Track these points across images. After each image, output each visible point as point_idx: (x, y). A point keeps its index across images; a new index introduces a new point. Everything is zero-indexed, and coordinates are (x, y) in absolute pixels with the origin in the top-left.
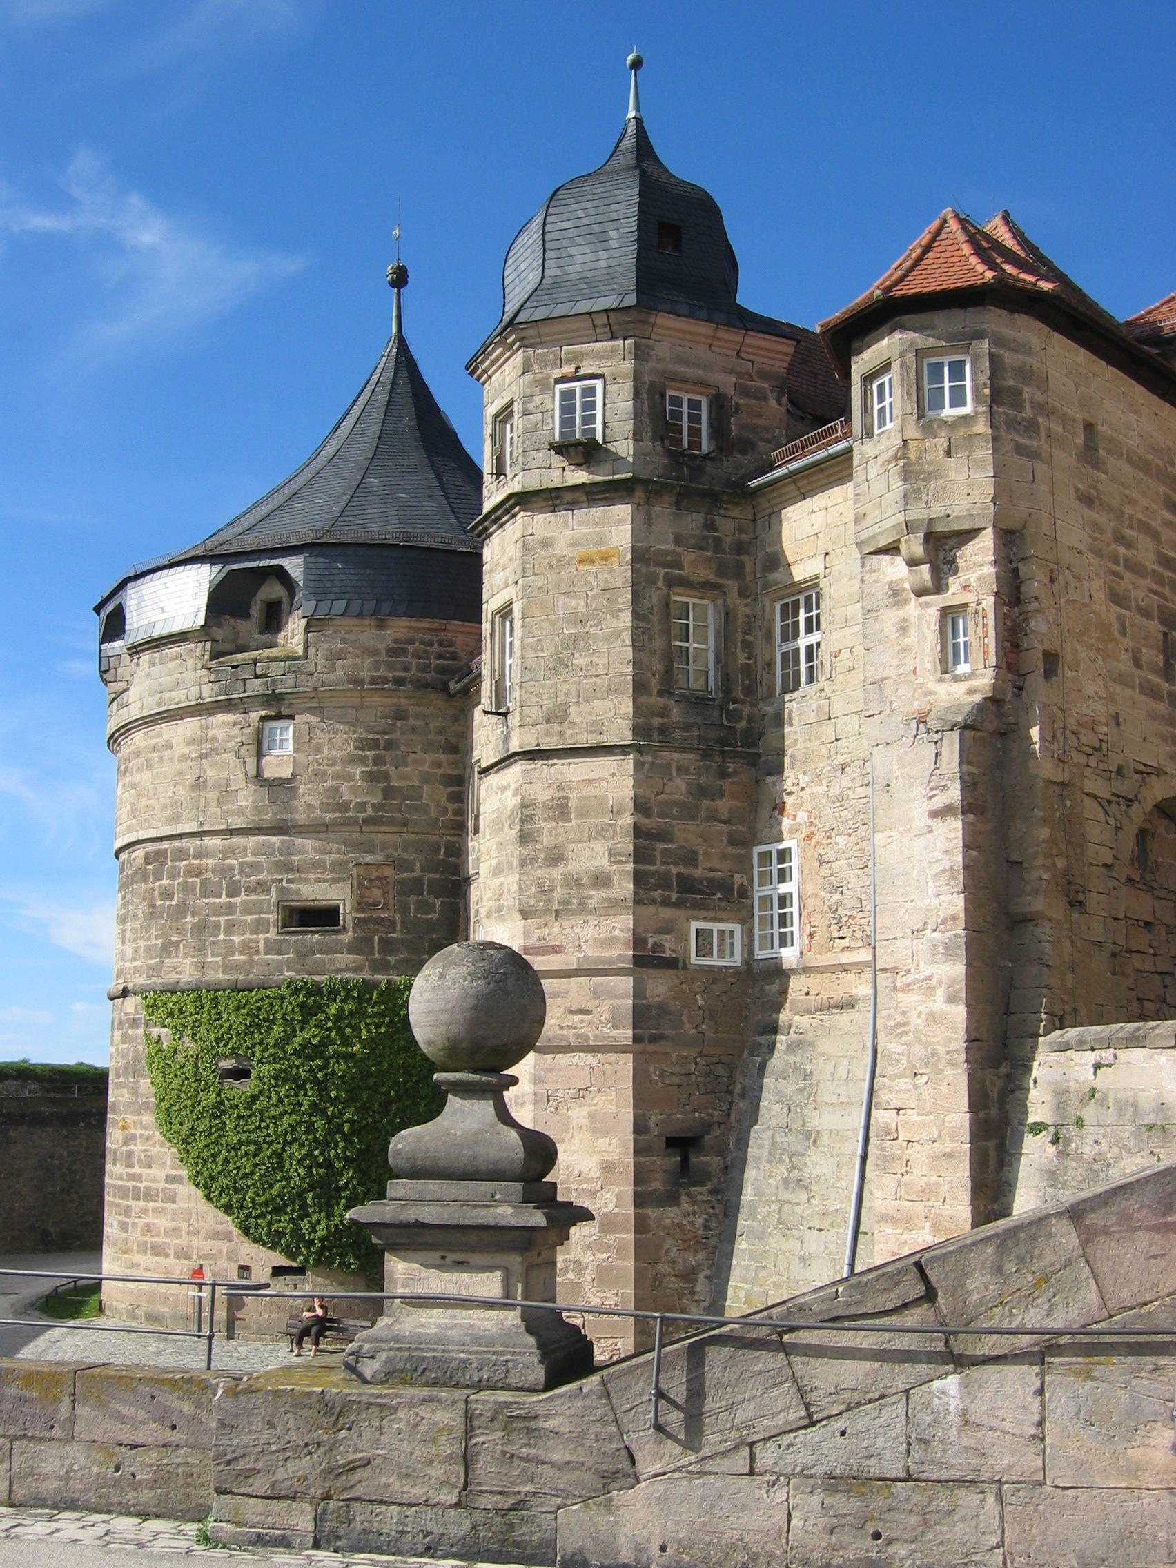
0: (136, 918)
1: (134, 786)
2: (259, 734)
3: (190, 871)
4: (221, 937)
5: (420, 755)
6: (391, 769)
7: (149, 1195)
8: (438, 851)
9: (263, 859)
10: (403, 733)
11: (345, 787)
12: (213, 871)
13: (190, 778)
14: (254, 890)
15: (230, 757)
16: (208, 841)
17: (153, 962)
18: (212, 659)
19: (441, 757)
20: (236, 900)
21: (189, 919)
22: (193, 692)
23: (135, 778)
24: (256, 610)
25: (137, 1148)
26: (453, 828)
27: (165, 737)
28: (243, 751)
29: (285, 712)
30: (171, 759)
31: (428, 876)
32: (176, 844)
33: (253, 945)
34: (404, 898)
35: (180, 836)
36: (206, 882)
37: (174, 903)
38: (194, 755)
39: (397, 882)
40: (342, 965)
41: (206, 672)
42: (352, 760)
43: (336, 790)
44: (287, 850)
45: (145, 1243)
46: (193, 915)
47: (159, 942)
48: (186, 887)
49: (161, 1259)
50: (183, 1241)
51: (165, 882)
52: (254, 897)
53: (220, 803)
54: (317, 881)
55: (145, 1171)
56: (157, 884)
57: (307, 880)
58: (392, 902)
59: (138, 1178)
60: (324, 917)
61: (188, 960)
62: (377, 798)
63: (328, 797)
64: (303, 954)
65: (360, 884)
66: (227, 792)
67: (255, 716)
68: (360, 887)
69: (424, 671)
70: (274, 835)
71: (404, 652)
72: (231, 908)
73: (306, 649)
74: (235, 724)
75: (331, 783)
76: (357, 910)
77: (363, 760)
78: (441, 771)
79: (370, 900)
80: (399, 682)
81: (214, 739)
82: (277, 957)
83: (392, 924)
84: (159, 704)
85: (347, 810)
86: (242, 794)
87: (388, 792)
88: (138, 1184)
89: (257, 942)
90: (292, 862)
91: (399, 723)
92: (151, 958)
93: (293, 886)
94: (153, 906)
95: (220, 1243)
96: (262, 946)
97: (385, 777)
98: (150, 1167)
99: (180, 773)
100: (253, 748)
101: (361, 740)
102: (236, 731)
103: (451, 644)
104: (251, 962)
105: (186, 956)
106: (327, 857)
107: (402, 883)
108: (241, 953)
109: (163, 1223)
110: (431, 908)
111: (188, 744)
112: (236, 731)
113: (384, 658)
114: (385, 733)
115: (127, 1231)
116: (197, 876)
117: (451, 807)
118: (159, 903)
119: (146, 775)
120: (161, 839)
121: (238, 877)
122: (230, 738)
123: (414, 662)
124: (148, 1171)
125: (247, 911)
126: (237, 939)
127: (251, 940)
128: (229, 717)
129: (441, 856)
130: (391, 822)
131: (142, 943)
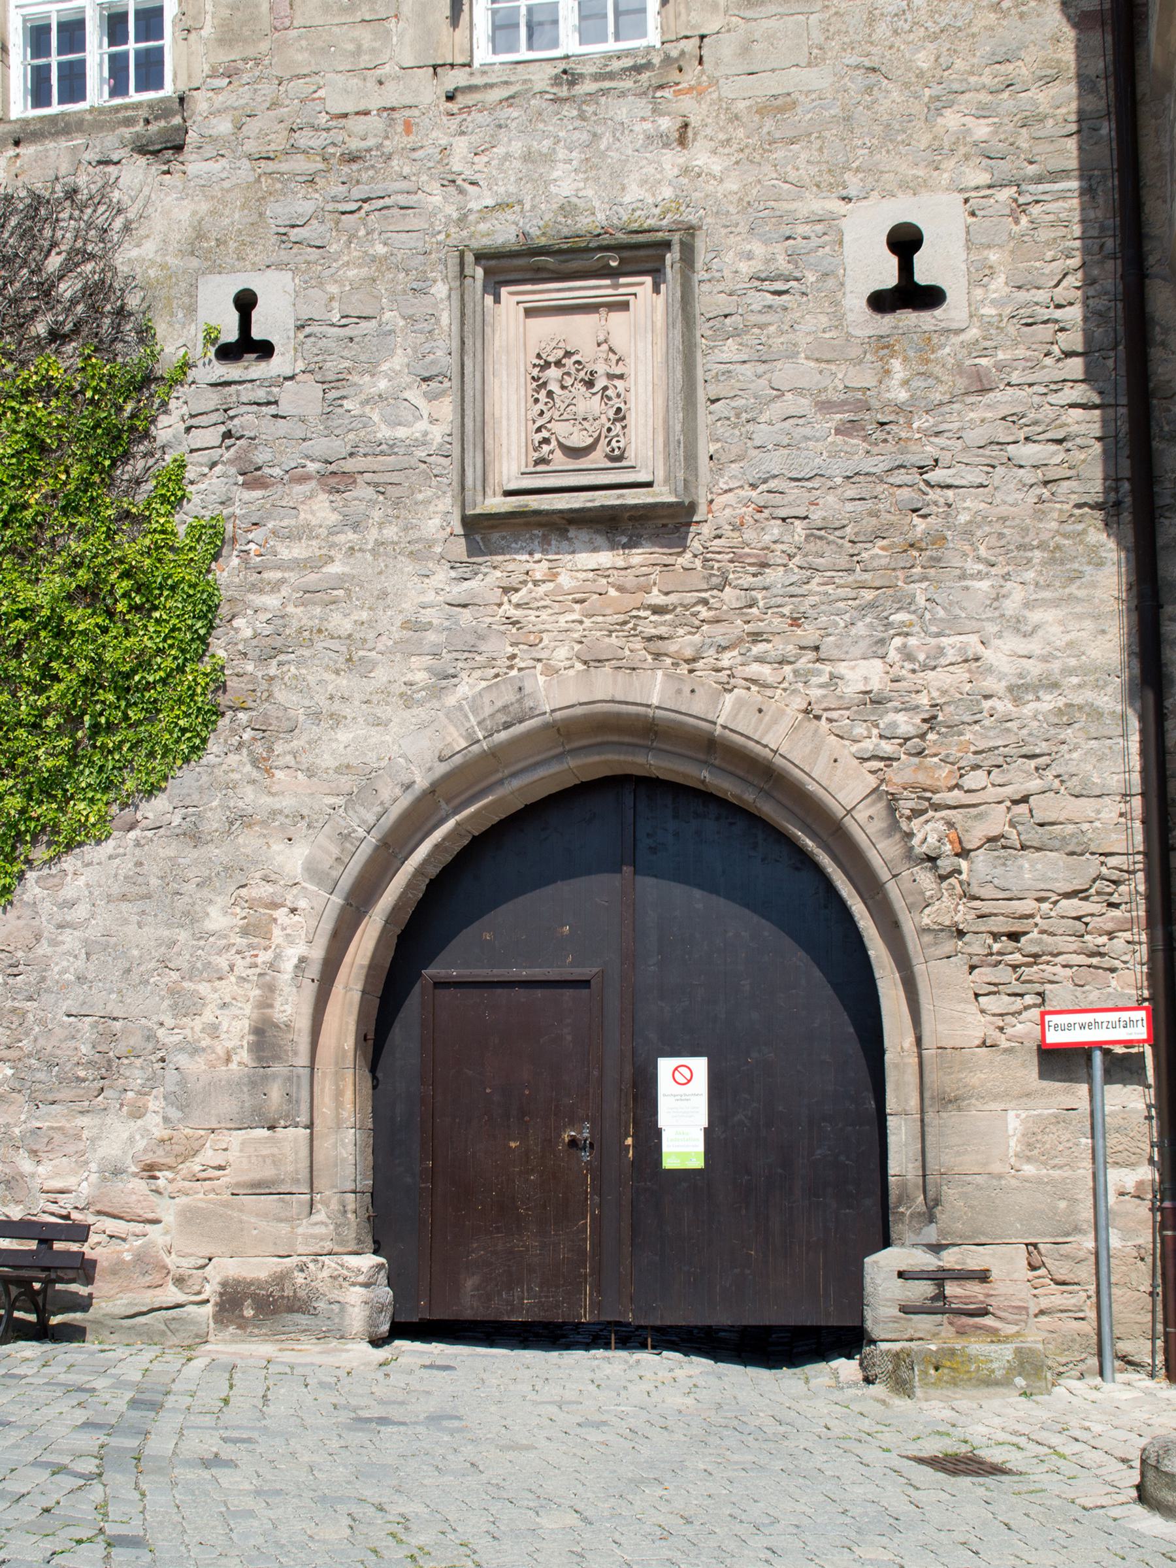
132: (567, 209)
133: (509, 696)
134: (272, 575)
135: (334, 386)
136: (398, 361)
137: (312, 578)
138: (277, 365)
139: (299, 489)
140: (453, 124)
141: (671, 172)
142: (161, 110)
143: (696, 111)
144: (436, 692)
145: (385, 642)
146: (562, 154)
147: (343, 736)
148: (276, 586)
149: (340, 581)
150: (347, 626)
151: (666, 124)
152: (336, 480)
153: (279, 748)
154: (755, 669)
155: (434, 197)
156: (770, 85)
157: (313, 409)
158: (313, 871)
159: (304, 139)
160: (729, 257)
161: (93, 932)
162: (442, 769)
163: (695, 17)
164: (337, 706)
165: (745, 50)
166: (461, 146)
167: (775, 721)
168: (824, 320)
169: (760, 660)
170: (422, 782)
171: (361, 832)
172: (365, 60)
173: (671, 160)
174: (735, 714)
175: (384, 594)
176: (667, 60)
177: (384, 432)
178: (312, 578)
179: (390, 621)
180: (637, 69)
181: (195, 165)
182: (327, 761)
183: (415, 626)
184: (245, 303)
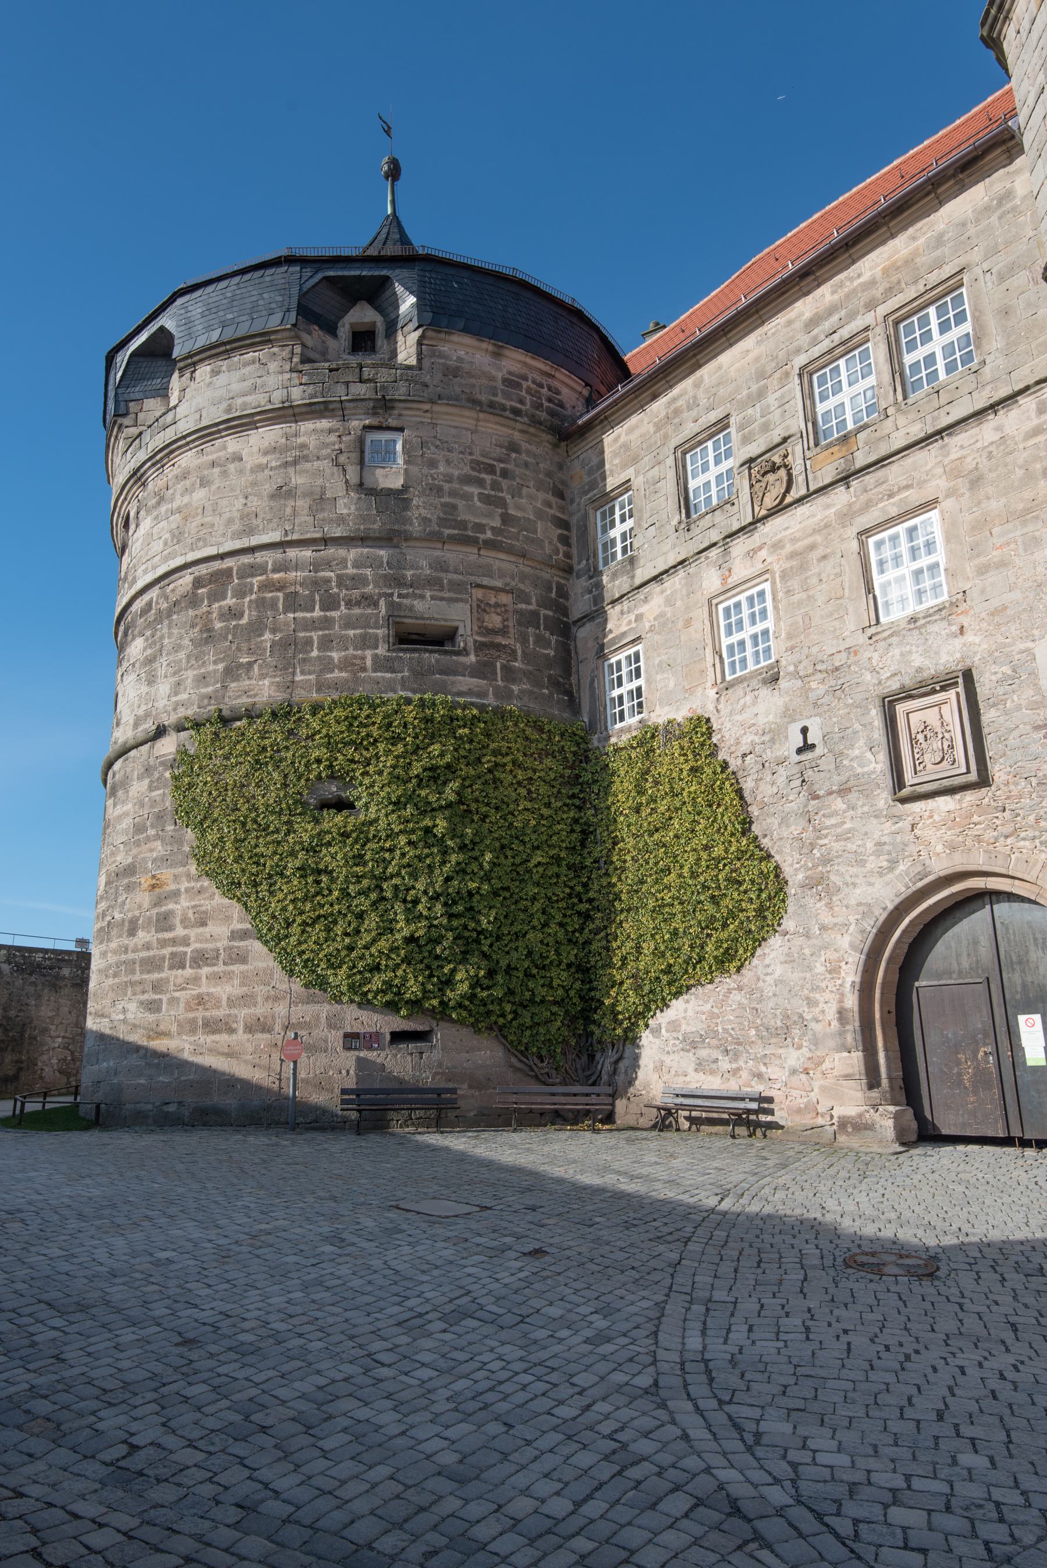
0: (177, 648)
1: (179, 510)
2: (361, 441)
3: (264, 587)
4: (315, 653)
5: (533, 491)
6: (508, 497)
7: (201, 959)
8: (550, 589)
9: (368, 572)
10: (517, 466)
11: (461, 504)
12: (301, 585)
13: (269, 488)
14: (358, 603)
15: (325, 465)
16: (292, 553)
17: (210, 689)
18: (303, 362)
19: (550, 497)
20: (335, 614)
21: (267, 636)
22: (278, 397)
24: (344, 330)
25: (181, 906)
26: (564, 570)
27: (230, 450)
28: (342, 459)
29: (392, 422)
31: (543, 612)
32: (246, 559)
33: (358, 662)
34: (523, 629)
35: (252, 550)
36: (287, 596)
37: (244, 621)
38: (274, 464)
39: (516, 611)
40: (464, 688)
41: (295, 375)
42: (466, 480)
43: (454, 507)
44: (397, 564)
45: (194, 1021)
46: (274, 631)
47: (221, 667)
48: (261, 604)
49: (223, 1038)
50: (260, 1010)
51: (230, 601)
52: (357, 611)
53: (312, 512)
54: (432, 598)
55: (193, 933)
56: (216, 605)
57: (422, 597)
58: (512, 630)
59: (185, 941)
60: (441, 639)
61: (266, 682)
62: (497, 523)
63: (445, 513)
64: (420, 673)
65: (479, 606)
66: (320, 501)
67: (356, 424)
68: (482, 608)
69: (537, 408)
70: (381, 547)
71: (518, 386)
72: (326, 623)
73: (420, 360)
74: (330, 431)
75: (446, 499)
76: (478, 634)
77: (481, 483)
78: (552, 512)
79: (490, 626)
80: (516, 412)
81: (303, 446)
82: (388, 675)
83: (514, 652)
84: (229, 410)
85: (465, 529)
86: (340, 503)
87: (506, 519)
88: (181, 949)
89: (363, 658)
90: (404, 576)
91: (514, 455)
92: (207, 686)
93: (406, 601)
95: (317, 1007)
96: (369, 662)
97: (503, 504)
98: (203, 924)
99: (254, 484)
100: (354, 456)
101: (478, 463)
102: (333, 438)
103: (558, 393)
104: (356, 680)
105: (262, 676)
106: (443, 575)
107: (520, 612)
108: (341, 670)
109: (224, 991)
110: (548, 645)
111: (266, 453)
112: (333, 438)
113: (499, 384)
114: (500, 461)
115: (158, 1010)
116: (278, 590)
117: (562, 548)
118: (218, 625)
120: (222, 557)
121: (335, 590)
122: (326, 445)
123: (528, 397)
124: (201, 930)
125: (348, 625)
126: (335, 655)
127: (355, 657)
128: (324, 424)
129: (553, 595)
130: (510, 550)
131: (190, 674)
132: (919, 670)
133: (920, 868)
134: (824, 832)
135: (838, 756)
136: (861, 743)
137: (839, 830)
138: (819, 751)
139: (831, 798)
140: (872, 648)
141: (958, 647)
142: (770, 667)
143: (965, 620)
144: (891, 869)
145: (869, 851)
146: (914, 649)
147: (858, 891)
148: (826, 836)
149: (849, 831)
150: (854, 848)
151: (955, 628)
152: (843, 791)
153: (834, 898)
154: (1022, 843)
155: (868, 676)
156: (995, 603)
157: (832, 766)
158: (852, 946)
159: (818, 667)
160: (987, 675)
161: (776, 976)
162: (897, 901)
163: (960, 585)
164: (853, 880)
165: (983, 591)
166: (876, 656)
167: (1034, 865)
168: (1031, 693)
169: (1024, 839)
170: (891, 907)
171: (869, 929)
172: (838, 633)
173: (958, 642)
174: (1016, 865)
175: (866, 834)
176: (952, 604)
177: (859, 770)
178: (839, 830)
179: (870, 845)
180: (940, 610)
181: (783, 683)
182: (853, 902)
183: (879, 844)
184: (804, 731)
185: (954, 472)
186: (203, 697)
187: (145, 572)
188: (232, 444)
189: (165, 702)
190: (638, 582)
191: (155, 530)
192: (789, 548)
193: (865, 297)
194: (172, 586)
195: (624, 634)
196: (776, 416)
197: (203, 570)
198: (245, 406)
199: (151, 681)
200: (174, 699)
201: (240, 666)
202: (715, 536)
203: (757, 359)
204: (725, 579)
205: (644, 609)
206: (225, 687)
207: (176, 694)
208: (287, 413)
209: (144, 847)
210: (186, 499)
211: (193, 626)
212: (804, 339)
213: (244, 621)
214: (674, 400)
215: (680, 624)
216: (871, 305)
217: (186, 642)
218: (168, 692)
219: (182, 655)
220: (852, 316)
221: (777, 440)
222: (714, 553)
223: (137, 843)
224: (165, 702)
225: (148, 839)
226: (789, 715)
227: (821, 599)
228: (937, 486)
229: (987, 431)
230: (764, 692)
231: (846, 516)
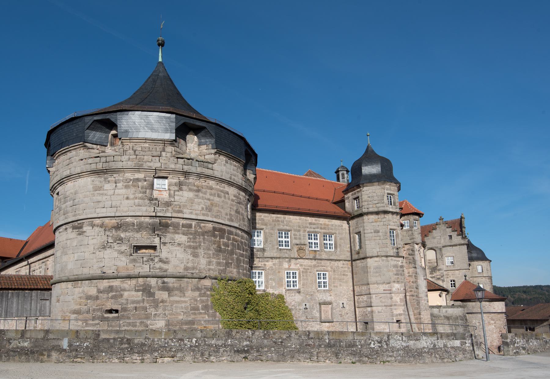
0: (209, 249)
1: (209, 199)
13: (235, 208)
17: (222, 268)
20: (244, 253)
21: (235, 256)
23: (208, 196)
30: (229, 199)
32: (229, 228)
48: (233, 245)
51: (225, 240)
56: (222, 240)
92: (220, 266)
94: (220, 248)
99: (232, 205)
111: (234, 196)
116: (236, 242)
118: (223, 247)
119: (216, 199)
120: (223, 224)
185: (332, 268)
186: (219, 270)
187: (191, 213)
188: (227, 188)
189: (204, 266)
190: (265, 256)
191: (195, 200)
192: (304, 267)
193: (320, 226)
194: (202, 225)
195: (260, 267)
196: (302, 238)
197: (217, 226)
198: (234, 180)
199: (195, 255)
200: (208, 267)
201: (229, 263)
202: (287, 256)
203: (299, 223)
204: (289, 267)
205: (267, 263)
206: (226, 269)
207: (209, 265)
208: (240, 188)
209: (198, 316)
210: (212, 198)
211: (214, 244)
212: (308, 225)
213: (229, 249)
214: (277, 217)
215: (277, 271)
216: (321, 228)
217: (212, 248)
218: (205, 263)
219: (211, 252)
220: (318, 228)
221: (302, 243)
222: (287, 260)
223: (195, 314)
224: (204, 266)
225: (201, 313)
226: (303, 301)
227: (309, 280)
228: (329, 268)
229: (336, 263)
230: (297, 294)
231: (315, 266)
